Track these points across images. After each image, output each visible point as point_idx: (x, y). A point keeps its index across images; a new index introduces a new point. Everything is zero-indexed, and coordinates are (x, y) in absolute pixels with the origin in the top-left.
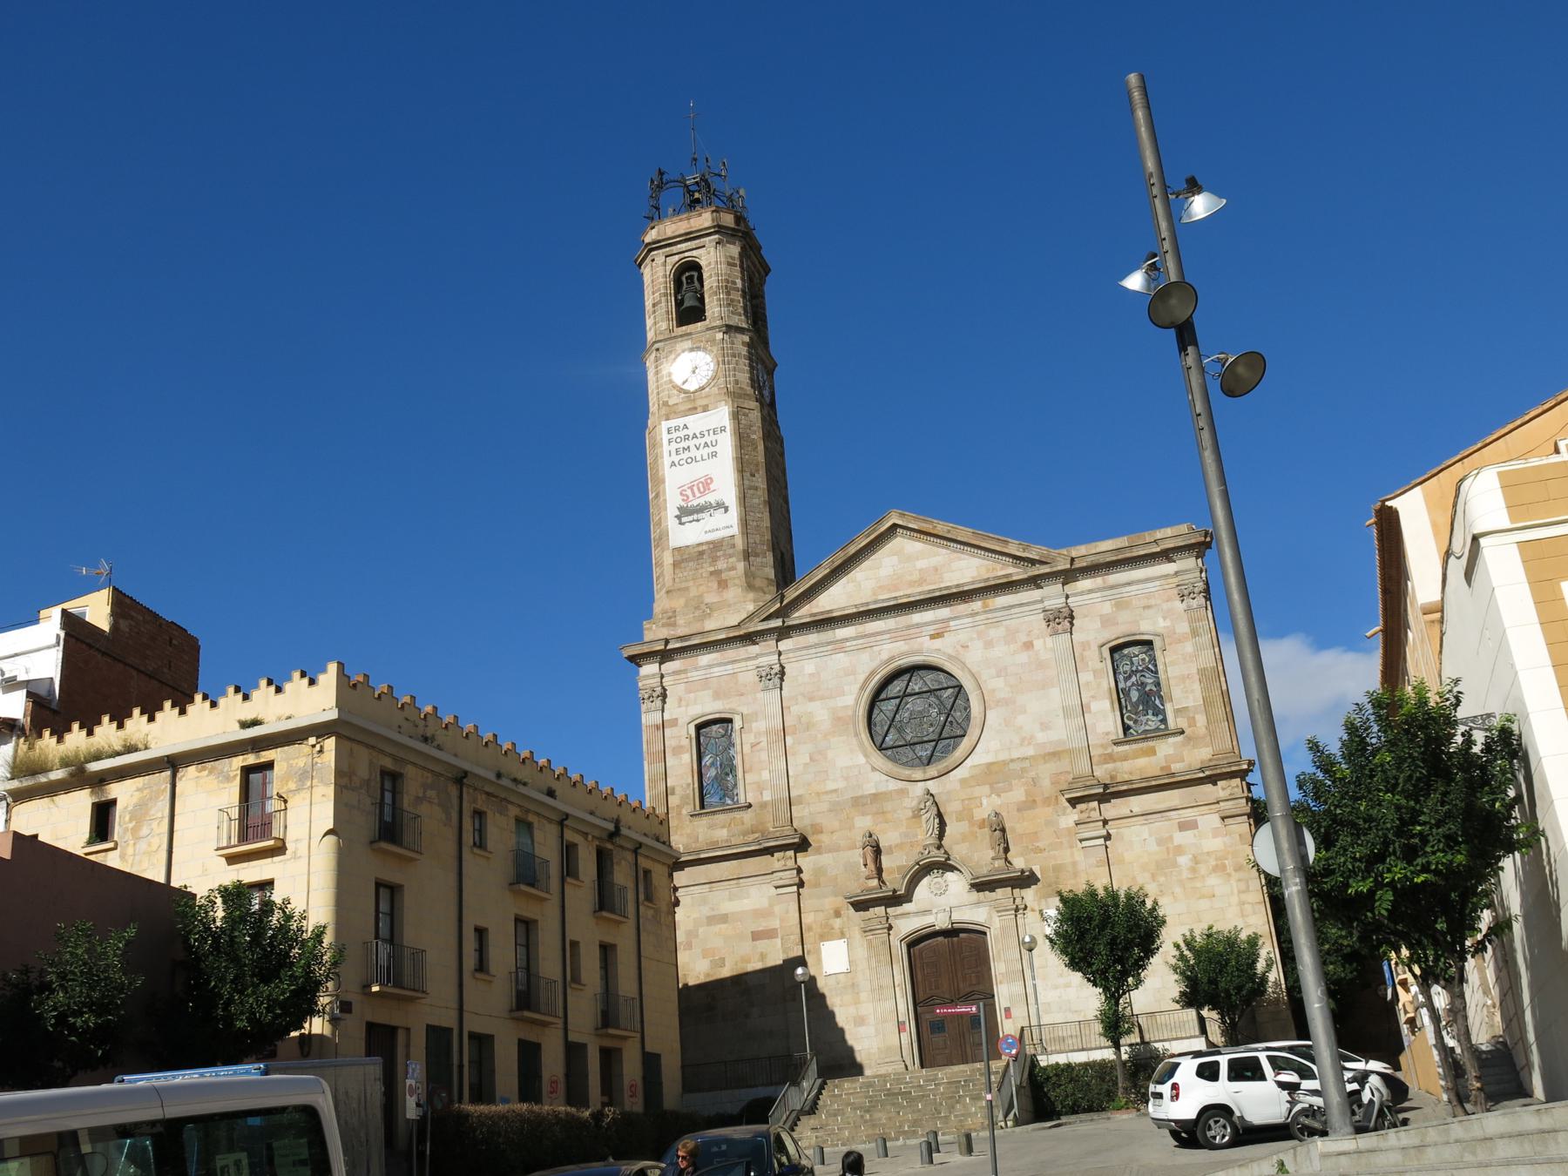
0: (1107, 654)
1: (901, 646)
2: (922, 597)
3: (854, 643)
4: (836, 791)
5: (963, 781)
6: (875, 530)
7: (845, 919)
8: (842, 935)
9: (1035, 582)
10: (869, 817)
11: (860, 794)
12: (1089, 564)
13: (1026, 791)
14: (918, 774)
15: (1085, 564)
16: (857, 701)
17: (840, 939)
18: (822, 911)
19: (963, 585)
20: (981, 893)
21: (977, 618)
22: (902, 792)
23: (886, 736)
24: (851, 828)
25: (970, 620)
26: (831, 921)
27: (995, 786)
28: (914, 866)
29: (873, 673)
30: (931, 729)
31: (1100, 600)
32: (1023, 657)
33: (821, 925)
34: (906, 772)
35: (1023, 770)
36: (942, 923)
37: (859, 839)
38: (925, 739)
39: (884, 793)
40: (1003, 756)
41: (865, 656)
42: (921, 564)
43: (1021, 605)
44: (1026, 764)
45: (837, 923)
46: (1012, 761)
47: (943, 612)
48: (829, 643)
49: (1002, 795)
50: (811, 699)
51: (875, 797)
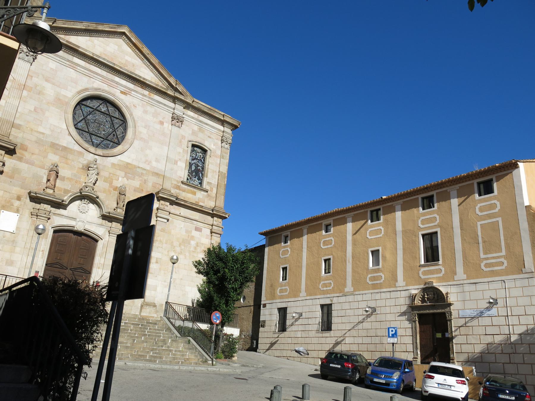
0: (190, 146)
1: (105, 87)
2: (126, 72)
3: (82, 69)
4: (43, 134)
5: (113, 165)
6: (115, 28)
7: (23, 203)
8: (17, 211)
9: (174, 99)
10: (58, 157)
11: (57, 142)
12: (198, 107)
13: (140, 183)
14: (92, 149)
15: (196, 106)
16: (73, 96)
17: (16, 213)
18: (9, 193)
19: (147, 80)
20: (104, 221)
21: (145, 98)
22: (80, 153)
23: (79, 122)
24: (45, 157)
25: (141, 96)
26: (13, 201)
27: (128, 175)
28: (78, 193)
29: (86, 90)
30: (103, 133)
31: (194, 123)
32: (158, 126)
33: (6, 201)
34: (86, 145)
35: (142, 174)
36: (79, 227)
37: (48, 165)
38: (98, 135)
39: (71, 150)
40: (135, 163)
41: (86, 79)
42: (127, 58)
43: (165, 105)
44: (144, 172)
45: (17, 203)
46: (139, 167)
47: (131, 85)
48: (68, 61)
49: (129, 180)
50: (47, 80)
51: (65, 149)
